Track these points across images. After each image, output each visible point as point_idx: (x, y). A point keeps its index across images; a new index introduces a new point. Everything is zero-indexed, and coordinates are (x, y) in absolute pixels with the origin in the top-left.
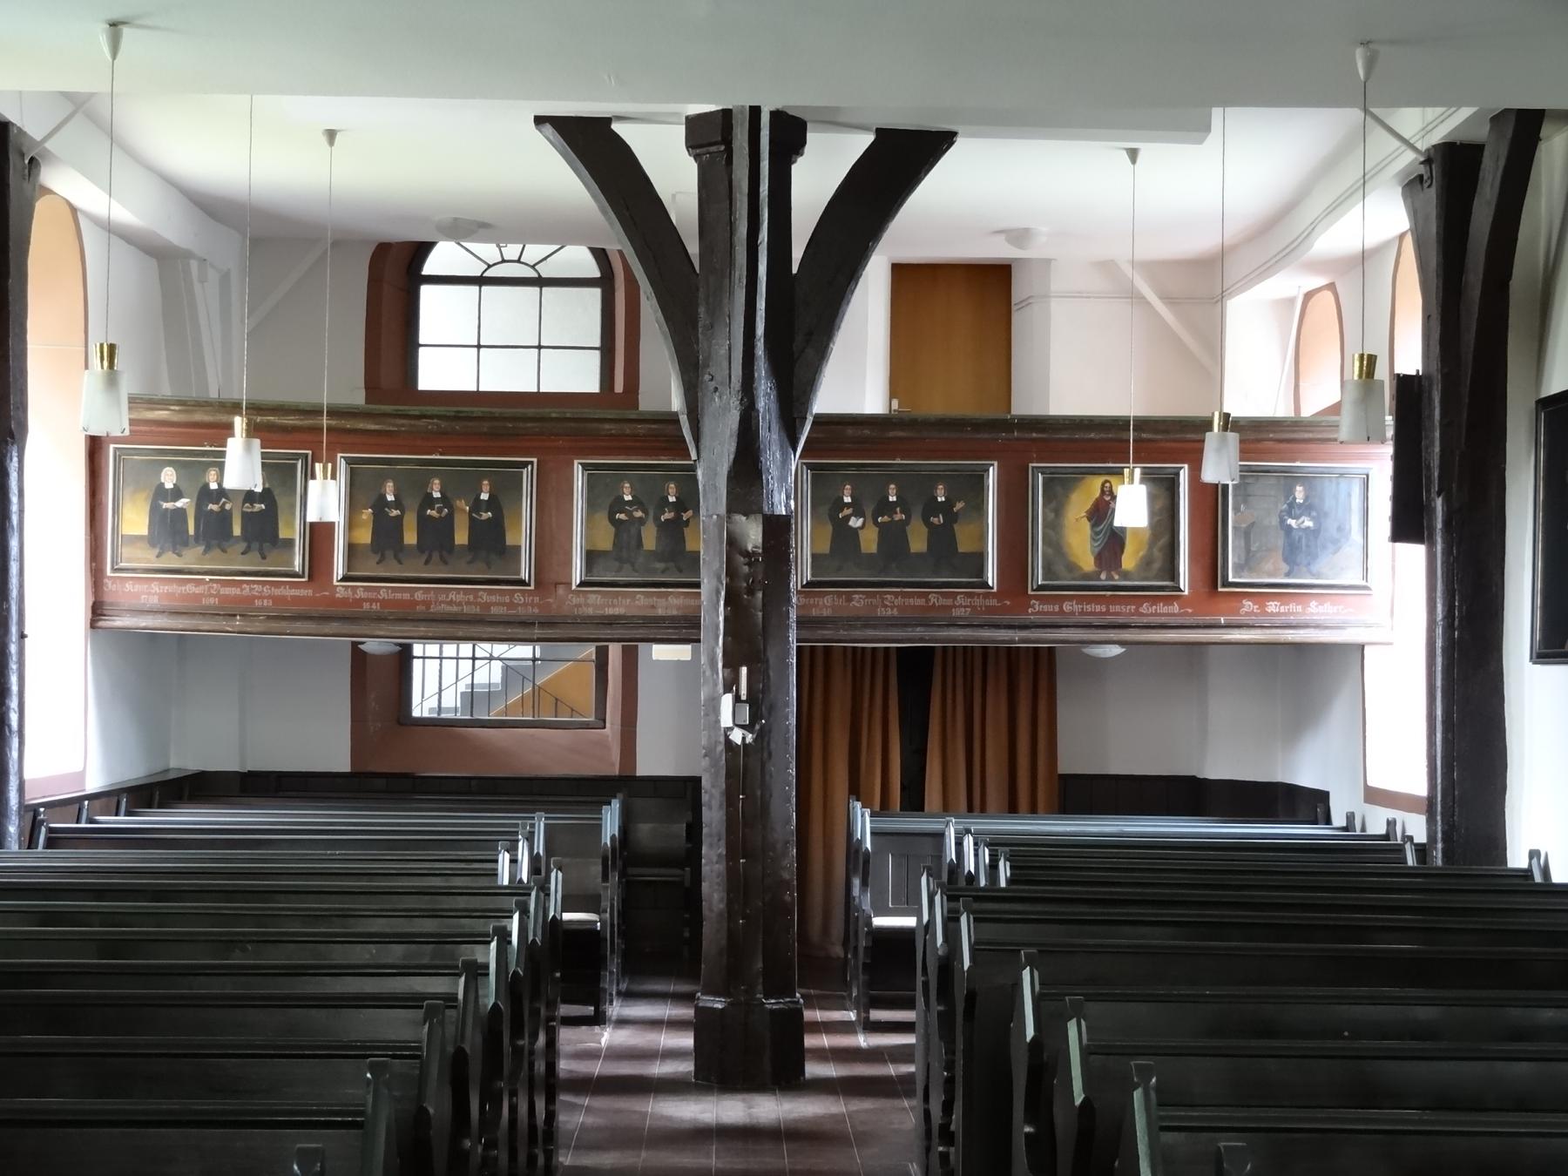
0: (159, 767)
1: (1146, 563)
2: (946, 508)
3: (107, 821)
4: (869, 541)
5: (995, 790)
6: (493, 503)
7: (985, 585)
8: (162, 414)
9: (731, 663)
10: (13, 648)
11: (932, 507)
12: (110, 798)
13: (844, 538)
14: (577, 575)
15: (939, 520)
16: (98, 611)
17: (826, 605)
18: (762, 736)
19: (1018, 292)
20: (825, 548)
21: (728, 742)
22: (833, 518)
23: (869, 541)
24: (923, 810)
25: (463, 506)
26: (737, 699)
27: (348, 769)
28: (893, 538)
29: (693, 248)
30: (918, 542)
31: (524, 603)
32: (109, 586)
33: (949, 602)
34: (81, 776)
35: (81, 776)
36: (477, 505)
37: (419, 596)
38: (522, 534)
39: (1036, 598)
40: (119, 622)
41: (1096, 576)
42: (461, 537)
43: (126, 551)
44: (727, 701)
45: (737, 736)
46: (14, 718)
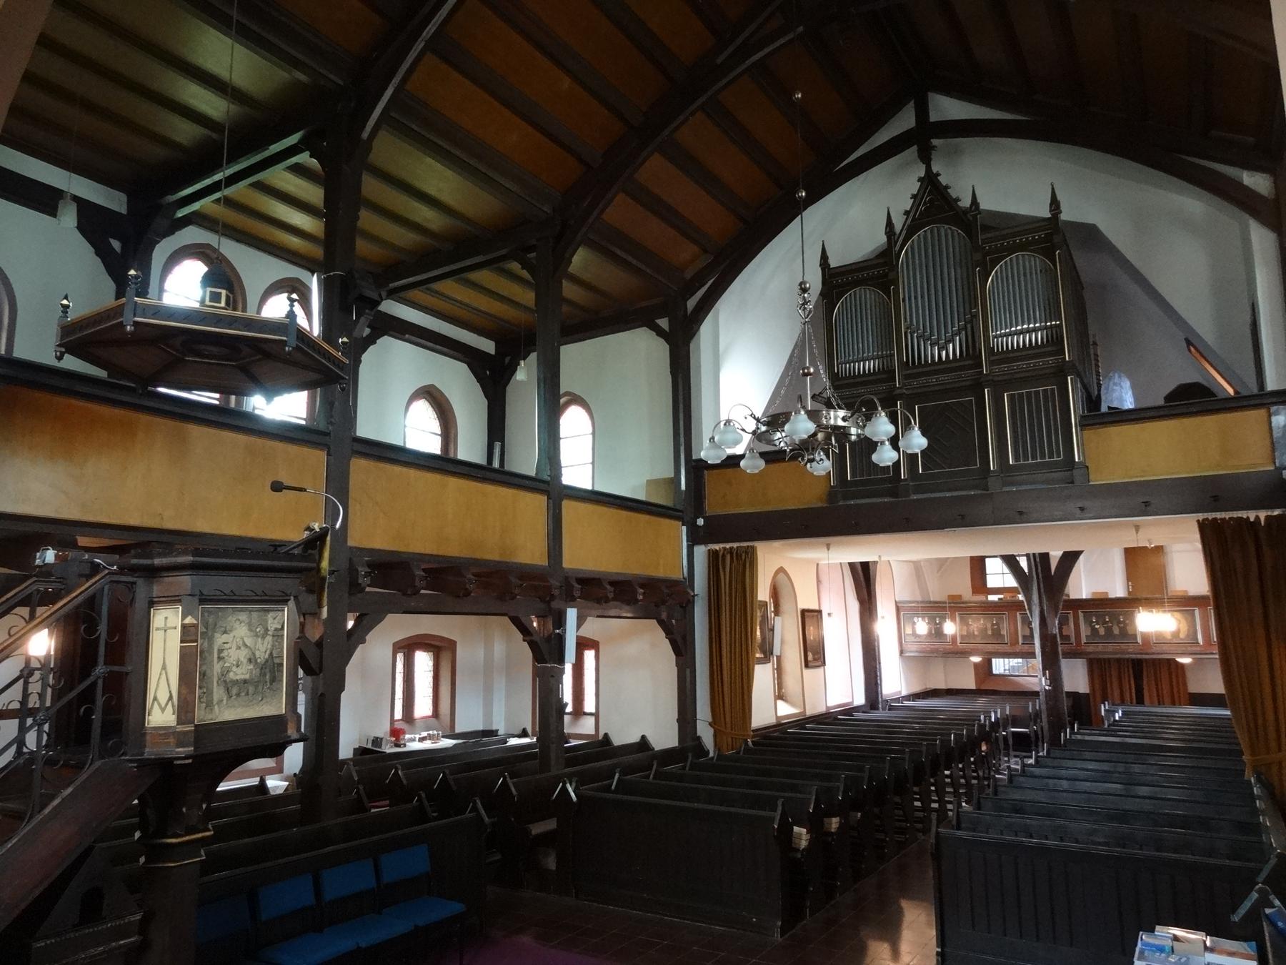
0: (924, 687)
1: (1188, 636)
2: (1124, 622)
3: (907, 703)
4: (1102, 632)
5: (1167, 699)
6: (997, 624)
7: (1137, 643)
8: (913, 605)
9: (1044, 669)
10: (878, 666)
11: (1119, 622)
12: (908, 698)
13: (1094, 631)
14: (1020, 644)
15: (1122, 625)
16: (902, 652)
17: (1090, 649)
18: (1053, 687)
19: (1165, 551)
20: (1089, 634)
21: (1045, 689)
22: (1091, 625)
23: (1102, 632)
24: (1143, 703)
25: (989, 626)
26: (1046, 679)
27: (974, 688)
28: (1108, 630)
29: (1026, 570)
30: (1116, 631)
31: (1007, 649)
32: (904, 646)
33: (1127, 647)
34: (900, 692)
35: (900, 692)
36: (993, 625)
37: (980, 647)
38: (1004, 632)
39: (1156, 646)
40: (907, 655)
41: (1170, 640)
42: (990, 632)
43: (907, 637)
44: (1043, 679)
45: (1047, 688)
46: (879, 681)
